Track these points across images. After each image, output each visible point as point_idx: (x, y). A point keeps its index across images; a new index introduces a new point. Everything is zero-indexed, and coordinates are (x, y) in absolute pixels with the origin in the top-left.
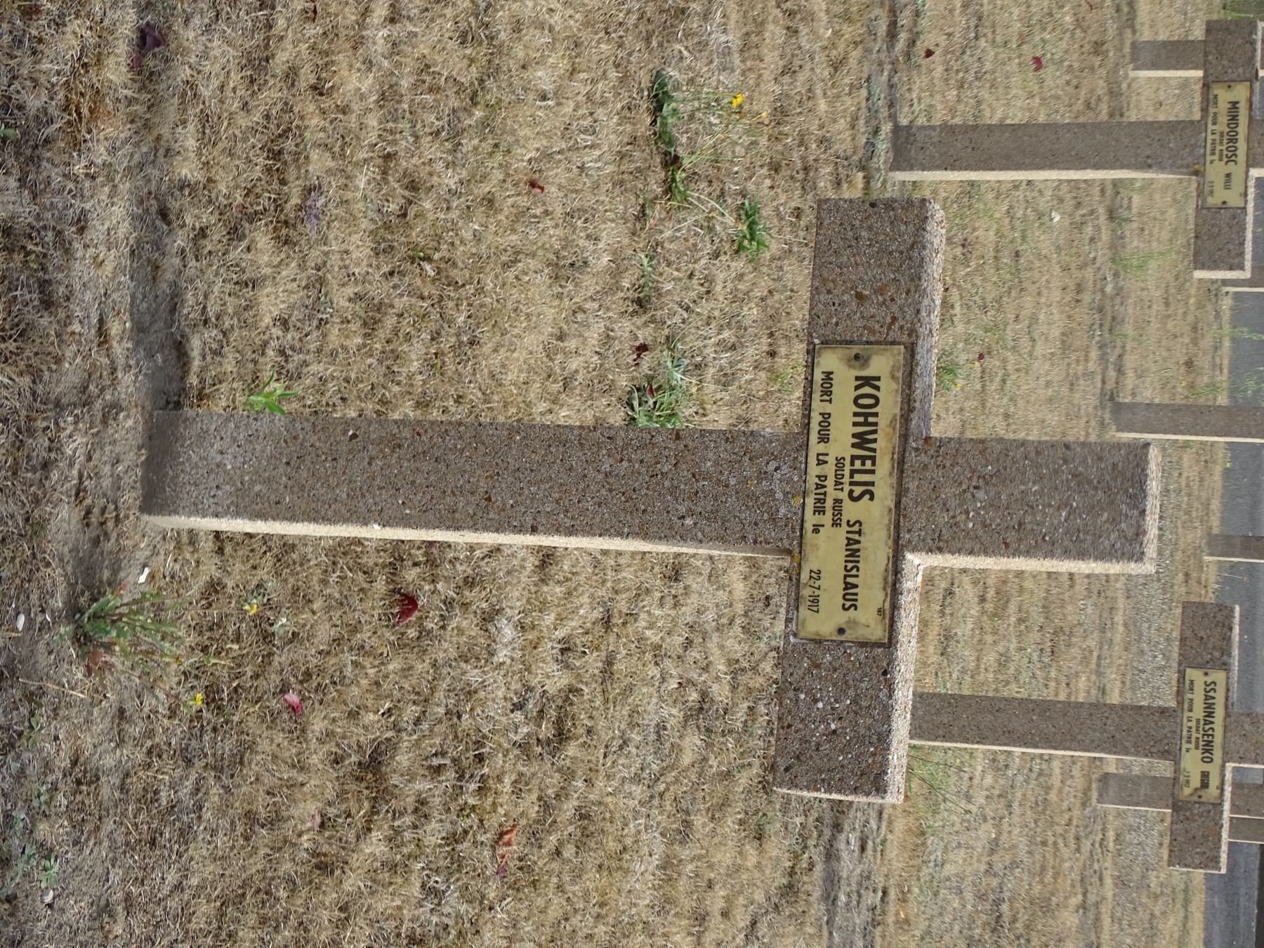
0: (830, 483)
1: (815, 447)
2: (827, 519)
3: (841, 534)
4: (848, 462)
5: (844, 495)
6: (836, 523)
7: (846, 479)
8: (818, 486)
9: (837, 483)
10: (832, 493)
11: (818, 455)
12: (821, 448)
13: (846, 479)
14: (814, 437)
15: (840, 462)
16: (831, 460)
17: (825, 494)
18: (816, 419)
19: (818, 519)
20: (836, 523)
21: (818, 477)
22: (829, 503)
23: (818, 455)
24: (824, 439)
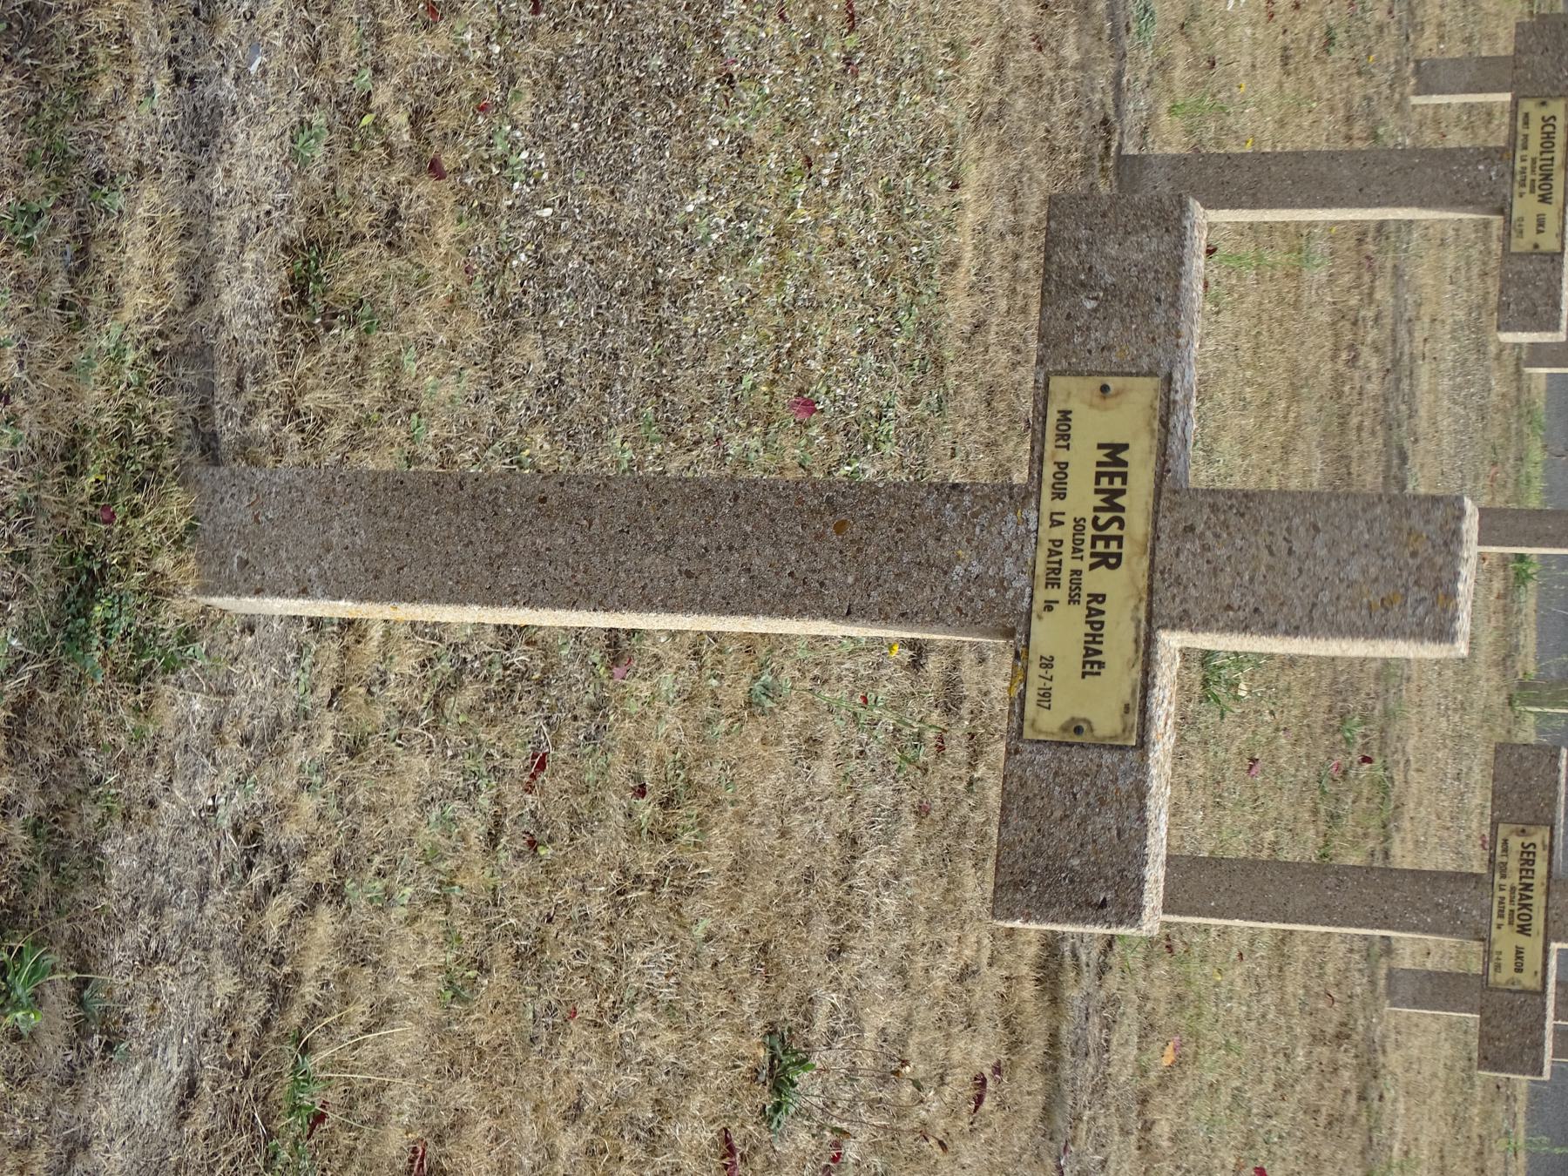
0: (1067, 549)
1: (1048, 504)
2: (1061, 594)
3: (1080, 611)
4: (1089, 524)
5: (1084, 565)
6: (1073, 600)
7: (1087, 546)
8: (1051, 553)
9: (1075, 550)
10: (1069, 564)
11: (1052, 514)
12: (1059, 505)
13: (1087, 546)
14: (1046, 492)
15: (1079, 524)
16: (1070, 524)
17: (1060, 562)
18: (1049, 470)
19: (1053, 594)
20: (1073, 600)
21: (1053, 541)
22: (1065, 577)
23: (1052, 514)
24: (1060, 495)
